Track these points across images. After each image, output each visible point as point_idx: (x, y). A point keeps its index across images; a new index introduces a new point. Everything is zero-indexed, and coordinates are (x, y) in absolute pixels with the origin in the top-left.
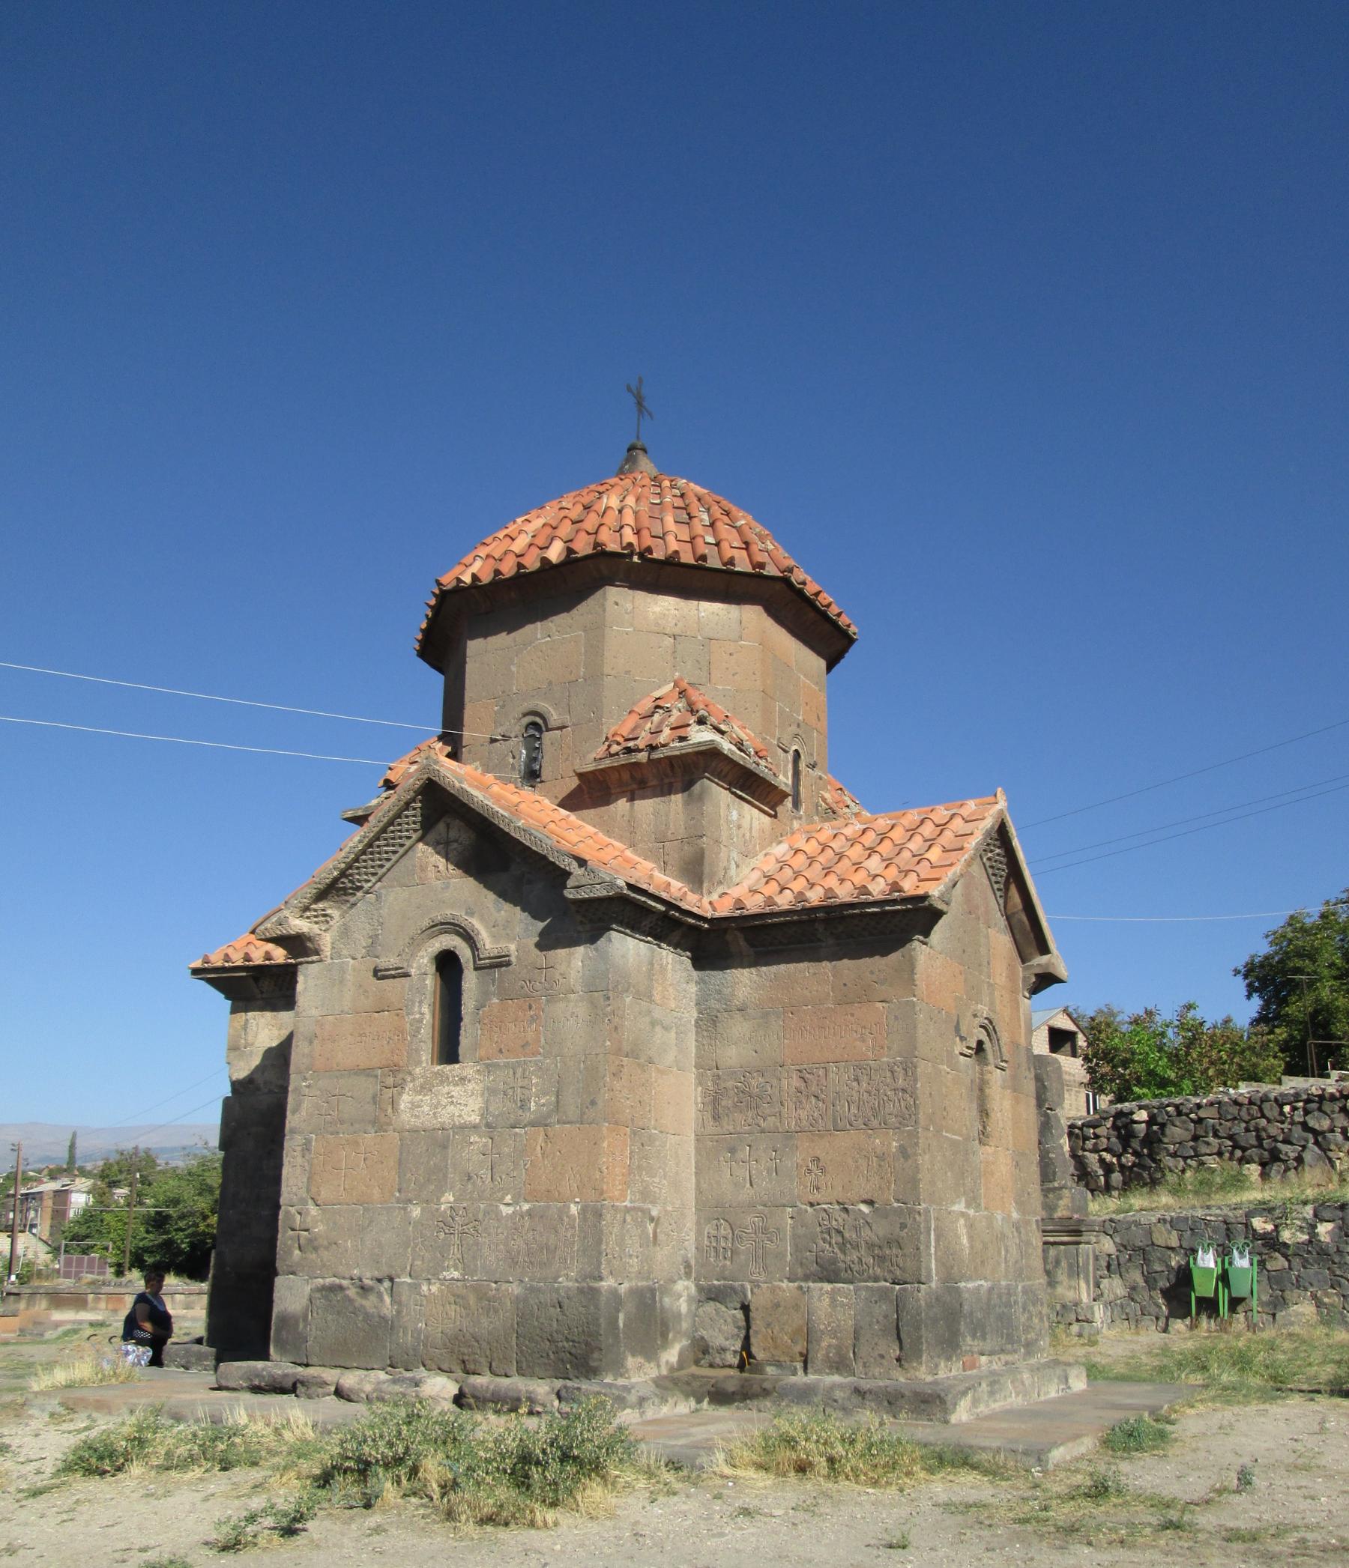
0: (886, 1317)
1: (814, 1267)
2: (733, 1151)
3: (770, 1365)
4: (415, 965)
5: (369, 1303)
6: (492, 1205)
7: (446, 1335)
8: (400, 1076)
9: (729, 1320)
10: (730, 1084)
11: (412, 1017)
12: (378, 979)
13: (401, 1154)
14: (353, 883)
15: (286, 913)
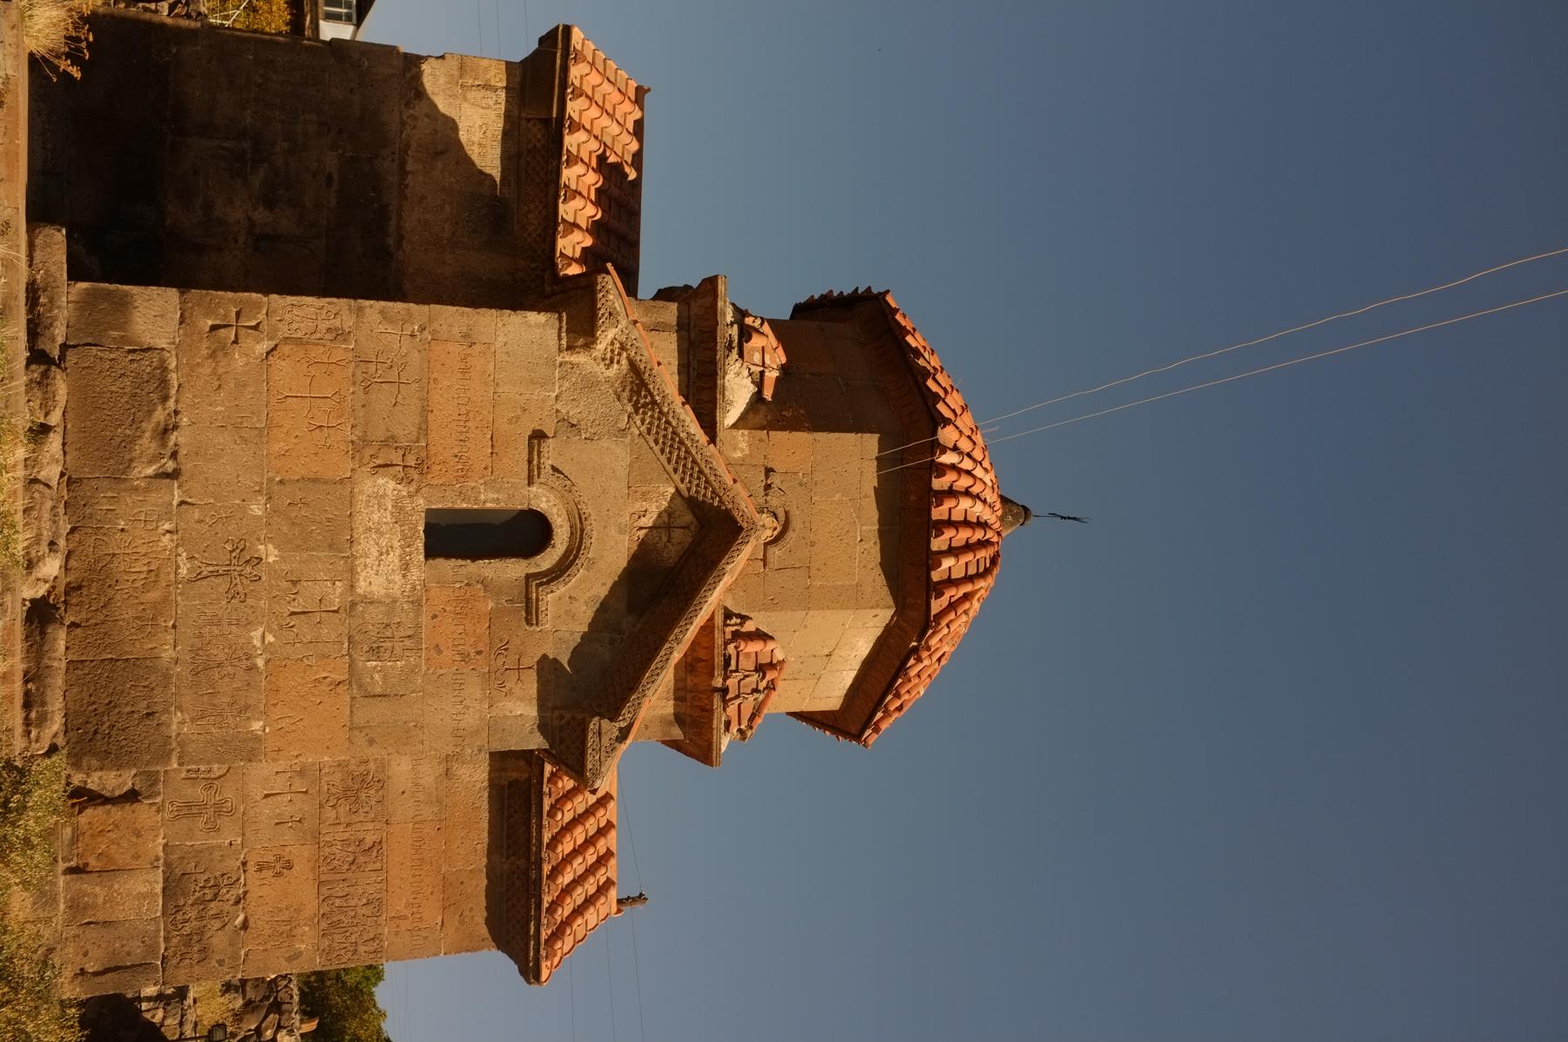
0: (129, 954)
1: (178, 872)
2: (302, 773)
3: (73, 829)
4: (540, 491)
5: (147, 444)
6: (264, 616)
7: (111, 562)
8: (416, 477)
9: (121, 780)
10: (372, 766)
11: (482, 487)
12: (530, 438)
13: (326, 482)
14: (643, 406)
15: (624, 323)
